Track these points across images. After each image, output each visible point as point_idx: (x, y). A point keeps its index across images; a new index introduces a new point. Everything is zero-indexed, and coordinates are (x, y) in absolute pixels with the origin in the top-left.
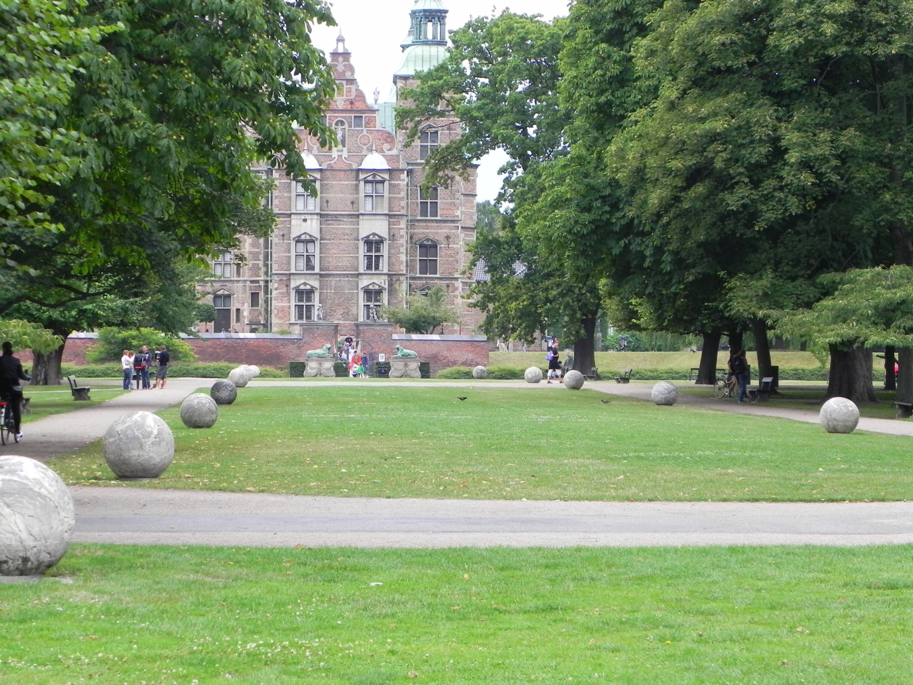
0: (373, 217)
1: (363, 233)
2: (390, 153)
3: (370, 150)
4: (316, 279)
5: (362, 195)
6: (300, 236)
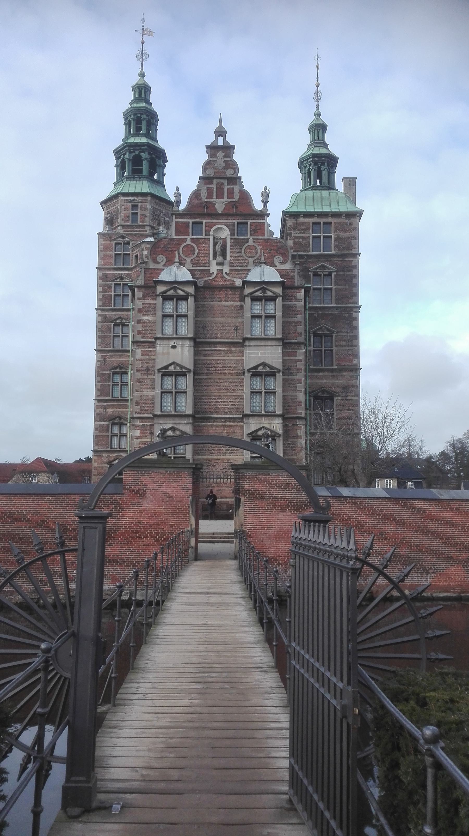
0: (263, 343)
1: (250, 363)
2: (283, 267)
3: (258, 263)
4: (187, 423)
5: (248, 315)
6: (167, 367)
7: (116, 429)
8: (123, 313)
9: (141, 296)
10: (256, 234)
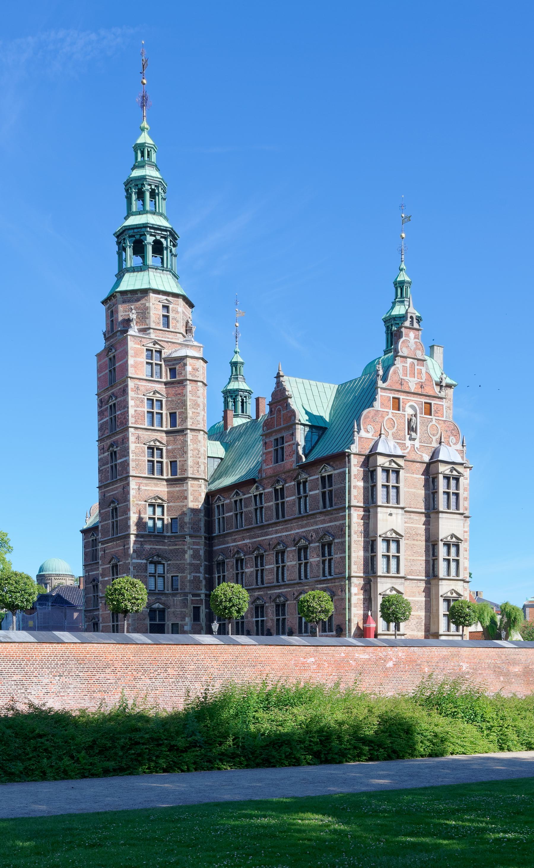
4: (401, 584)
7: (151, 568)
8: (156, 434)
9: (356, 463)
10: (437, 415)
